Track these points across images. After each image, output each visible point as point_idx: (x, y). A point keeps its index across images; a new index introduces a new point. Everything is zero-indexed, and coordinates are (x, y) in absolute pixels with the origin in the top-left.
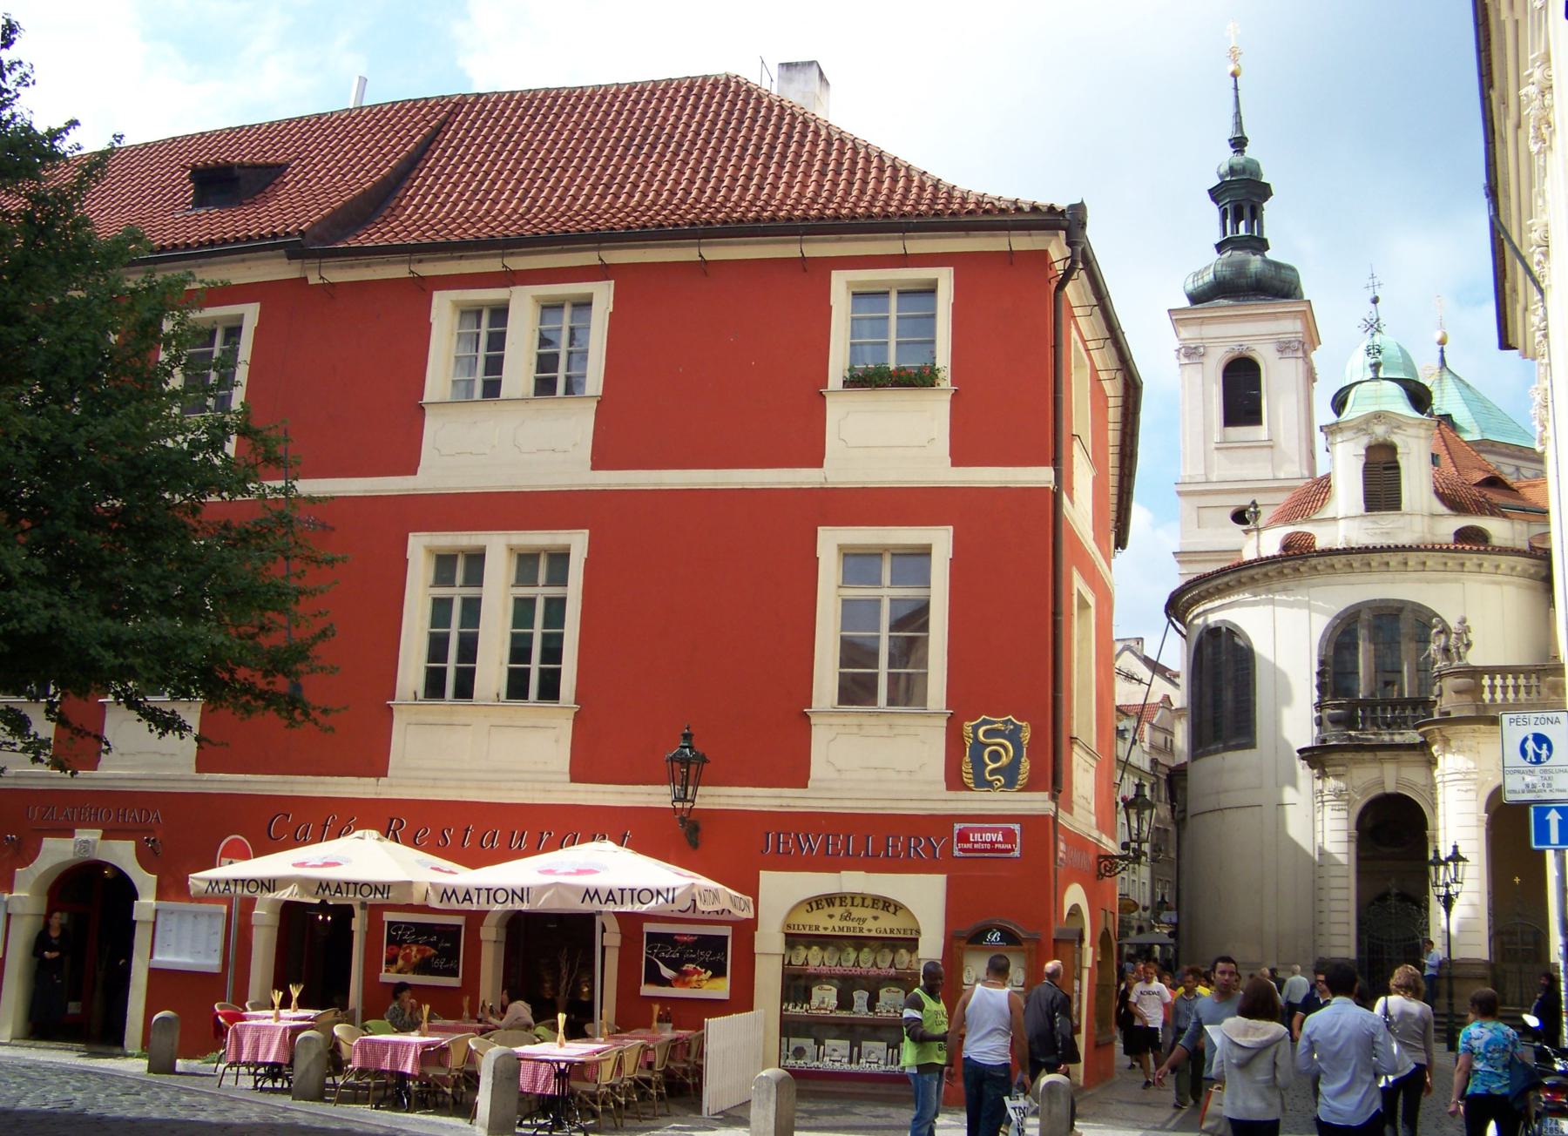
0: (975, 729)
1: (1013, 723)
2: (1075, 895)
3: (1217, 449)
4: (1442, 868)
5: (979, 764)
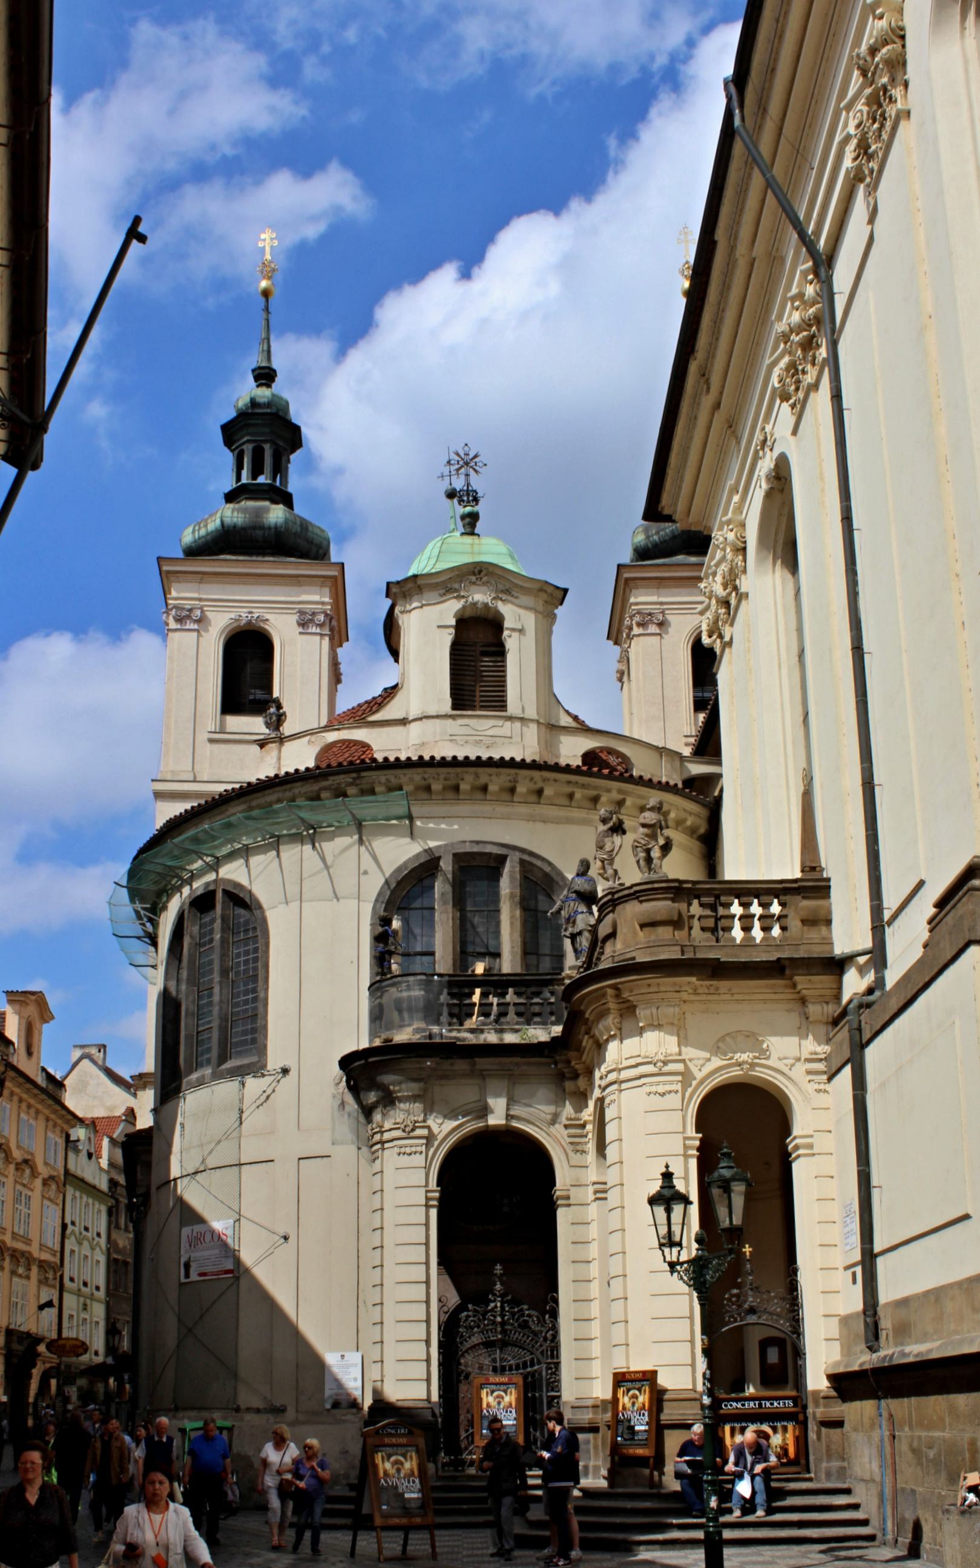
4: (678, 1209)
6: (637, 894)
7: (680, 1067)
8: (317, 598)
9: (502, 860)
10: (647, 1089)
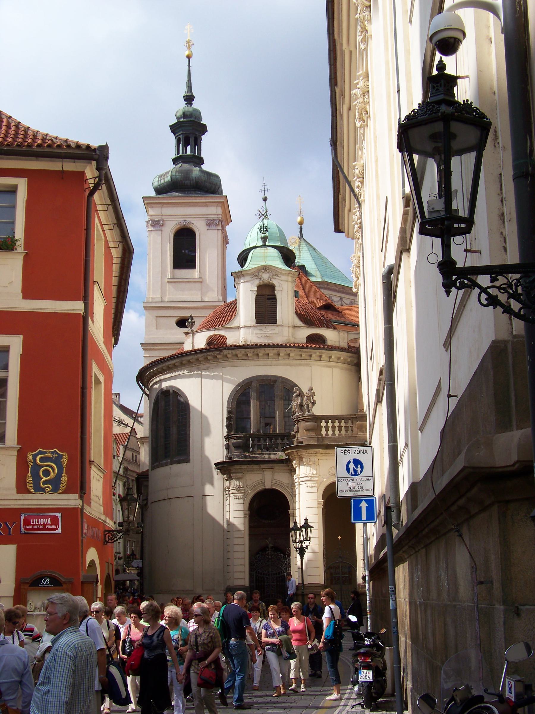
0: (35, 457)
1: (57, 453)
2: (92, 554)
3: (168, 282)
4: (298, 532)
5: (36, 478)
8: (215, 211)
10: (306, 485)
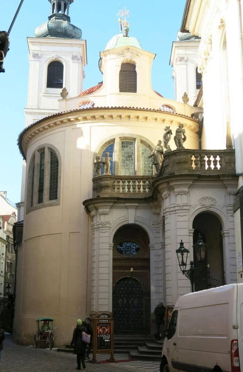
4: (185, 254)
6: (174, 153)
7: (188, 208)
9: (135, 139)
10: (178, 215)
